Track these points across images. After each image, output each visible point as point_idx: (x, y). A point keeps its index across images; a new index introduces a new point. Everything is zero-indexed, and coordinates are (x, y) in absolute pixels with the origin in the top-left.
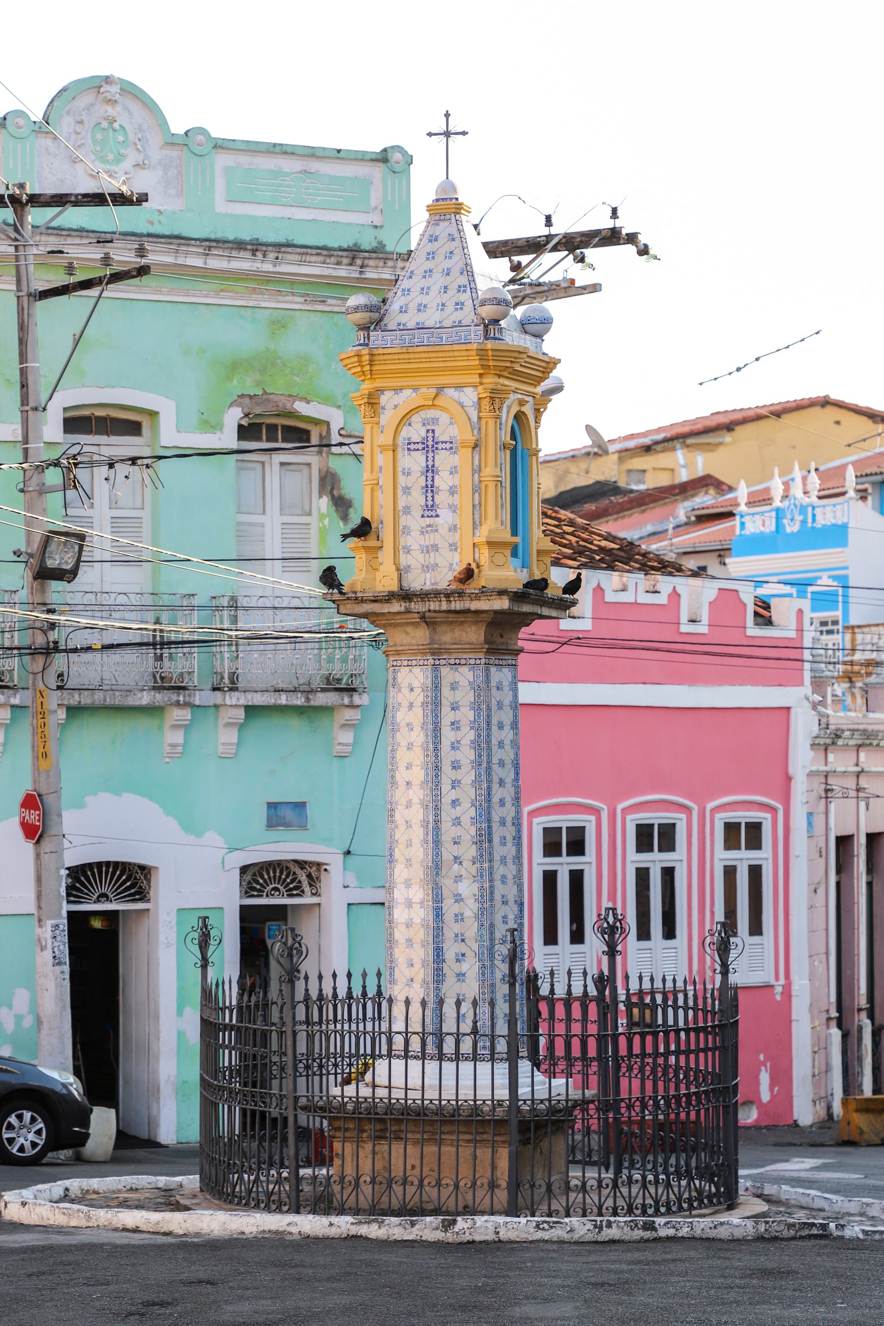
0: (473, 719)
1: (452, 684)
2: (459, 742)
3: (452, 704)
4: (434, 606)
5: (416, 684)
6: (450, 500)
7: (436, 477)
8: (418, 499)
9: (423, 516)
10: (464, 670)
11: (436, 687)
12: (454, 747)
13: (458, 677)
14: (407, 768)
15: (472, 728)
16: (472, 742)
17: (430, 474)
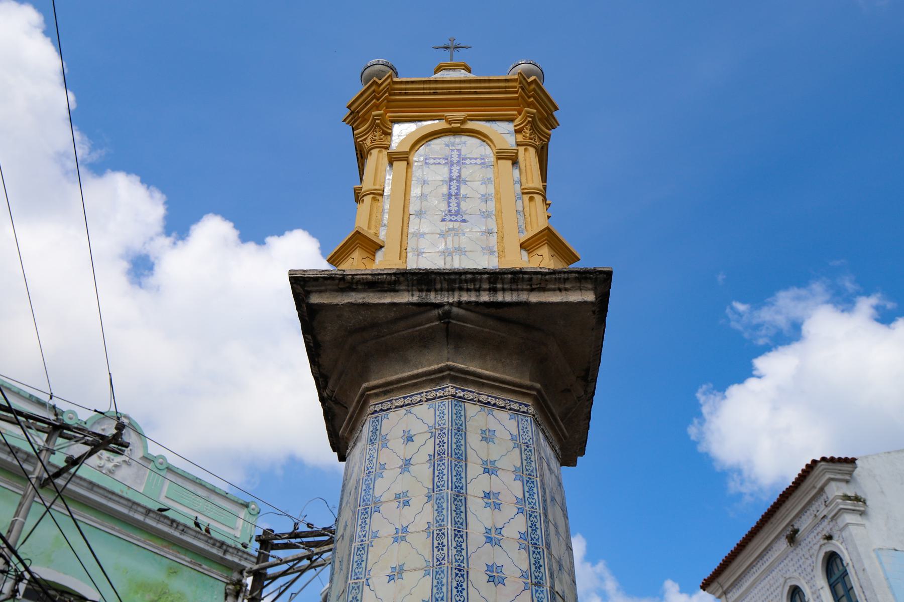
0: (521, 496)
1: (483, 432)
2: (499, 530)
3: (485, 462)
4: (465, 297)
5: (417, 428)
6: (483, 207)
7: (463, 187)
8: (438, 205)
9: (443, 220)
10: (504, 416)
11: (459, 430)
12: (492, 538)
13: (492, 424)
14: (391, 578)
15: (520, 511)
17: (454, 184)
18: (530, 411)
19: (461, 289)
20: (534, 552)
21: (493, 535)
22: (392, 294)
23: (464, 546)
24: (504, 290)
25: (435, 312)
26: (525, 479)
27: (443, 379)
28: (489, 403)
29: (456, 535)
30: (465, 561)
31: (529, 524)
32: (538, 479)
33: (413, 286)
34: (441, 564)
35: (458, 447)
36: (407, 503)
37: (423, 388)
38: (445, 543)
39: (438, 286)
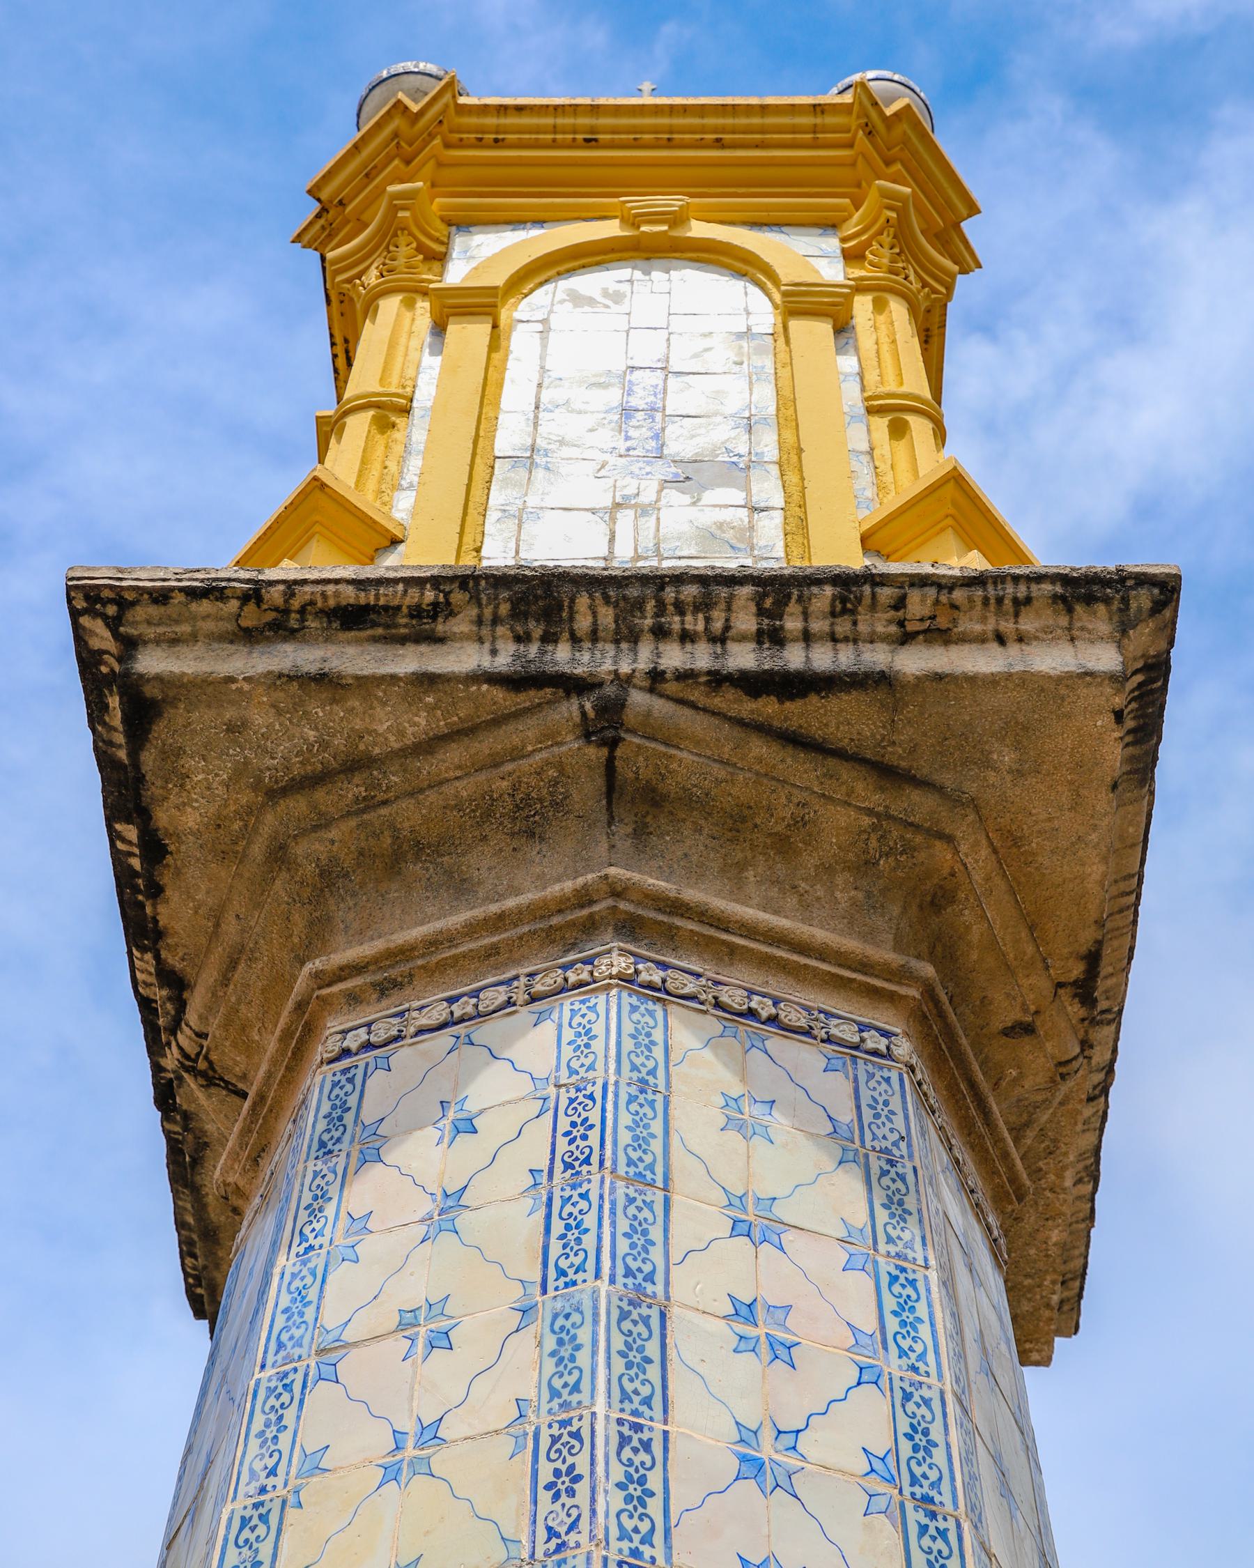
0: (869, 1324)
2: (790, 1437)
3: (735, 1201)
4: (673, 657)
15: (867, 1376)
16: (876, 1464)
18: (897, 1051)
19: (660, 633)
20: (923, 1529)
21: (767, 1449)
22: (423, 648)
23: (654, 1481)
24: (807, 638)
25: (570, 709)
26: (886, 1267)
27: (590, 927)
28: (751, 1013)
29: (624, 1441)
30: (658, 1538)
31: (904, 1427)
32: (933, 1276)
33: (496, 621)
34: (560, 1547)
35: (640, 1142)
36: (442, 1341)
37: (518, 962)
38: (582, 1468)
39: (583, 623)
